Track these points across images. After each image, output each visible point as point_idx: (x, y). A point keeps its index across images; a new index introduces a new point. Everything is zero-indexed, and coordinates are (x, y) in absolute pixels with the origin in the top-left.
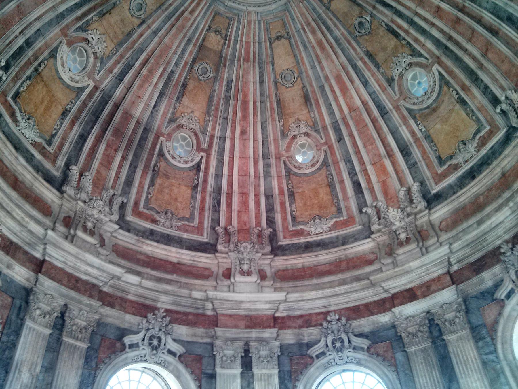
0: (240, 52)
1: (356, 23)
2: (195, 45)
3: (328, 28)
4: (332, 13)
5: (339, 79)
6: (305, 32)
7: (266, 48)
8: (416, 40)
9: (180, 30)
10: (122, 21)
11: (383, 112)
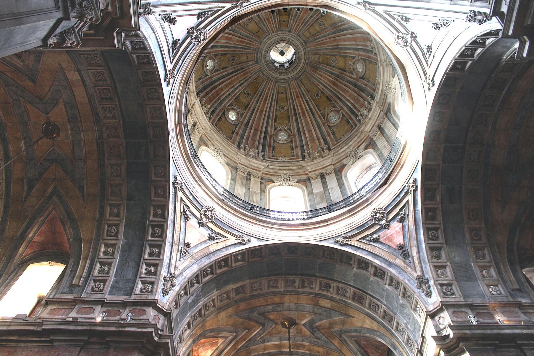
0: (272, 19)
1: (236, 58)
2: (293, 15)
4: (244, 54)
5: (230, 39)
7: (261, 26)
8: (218, 74)
9: (301, 19)
10: (326, 21)
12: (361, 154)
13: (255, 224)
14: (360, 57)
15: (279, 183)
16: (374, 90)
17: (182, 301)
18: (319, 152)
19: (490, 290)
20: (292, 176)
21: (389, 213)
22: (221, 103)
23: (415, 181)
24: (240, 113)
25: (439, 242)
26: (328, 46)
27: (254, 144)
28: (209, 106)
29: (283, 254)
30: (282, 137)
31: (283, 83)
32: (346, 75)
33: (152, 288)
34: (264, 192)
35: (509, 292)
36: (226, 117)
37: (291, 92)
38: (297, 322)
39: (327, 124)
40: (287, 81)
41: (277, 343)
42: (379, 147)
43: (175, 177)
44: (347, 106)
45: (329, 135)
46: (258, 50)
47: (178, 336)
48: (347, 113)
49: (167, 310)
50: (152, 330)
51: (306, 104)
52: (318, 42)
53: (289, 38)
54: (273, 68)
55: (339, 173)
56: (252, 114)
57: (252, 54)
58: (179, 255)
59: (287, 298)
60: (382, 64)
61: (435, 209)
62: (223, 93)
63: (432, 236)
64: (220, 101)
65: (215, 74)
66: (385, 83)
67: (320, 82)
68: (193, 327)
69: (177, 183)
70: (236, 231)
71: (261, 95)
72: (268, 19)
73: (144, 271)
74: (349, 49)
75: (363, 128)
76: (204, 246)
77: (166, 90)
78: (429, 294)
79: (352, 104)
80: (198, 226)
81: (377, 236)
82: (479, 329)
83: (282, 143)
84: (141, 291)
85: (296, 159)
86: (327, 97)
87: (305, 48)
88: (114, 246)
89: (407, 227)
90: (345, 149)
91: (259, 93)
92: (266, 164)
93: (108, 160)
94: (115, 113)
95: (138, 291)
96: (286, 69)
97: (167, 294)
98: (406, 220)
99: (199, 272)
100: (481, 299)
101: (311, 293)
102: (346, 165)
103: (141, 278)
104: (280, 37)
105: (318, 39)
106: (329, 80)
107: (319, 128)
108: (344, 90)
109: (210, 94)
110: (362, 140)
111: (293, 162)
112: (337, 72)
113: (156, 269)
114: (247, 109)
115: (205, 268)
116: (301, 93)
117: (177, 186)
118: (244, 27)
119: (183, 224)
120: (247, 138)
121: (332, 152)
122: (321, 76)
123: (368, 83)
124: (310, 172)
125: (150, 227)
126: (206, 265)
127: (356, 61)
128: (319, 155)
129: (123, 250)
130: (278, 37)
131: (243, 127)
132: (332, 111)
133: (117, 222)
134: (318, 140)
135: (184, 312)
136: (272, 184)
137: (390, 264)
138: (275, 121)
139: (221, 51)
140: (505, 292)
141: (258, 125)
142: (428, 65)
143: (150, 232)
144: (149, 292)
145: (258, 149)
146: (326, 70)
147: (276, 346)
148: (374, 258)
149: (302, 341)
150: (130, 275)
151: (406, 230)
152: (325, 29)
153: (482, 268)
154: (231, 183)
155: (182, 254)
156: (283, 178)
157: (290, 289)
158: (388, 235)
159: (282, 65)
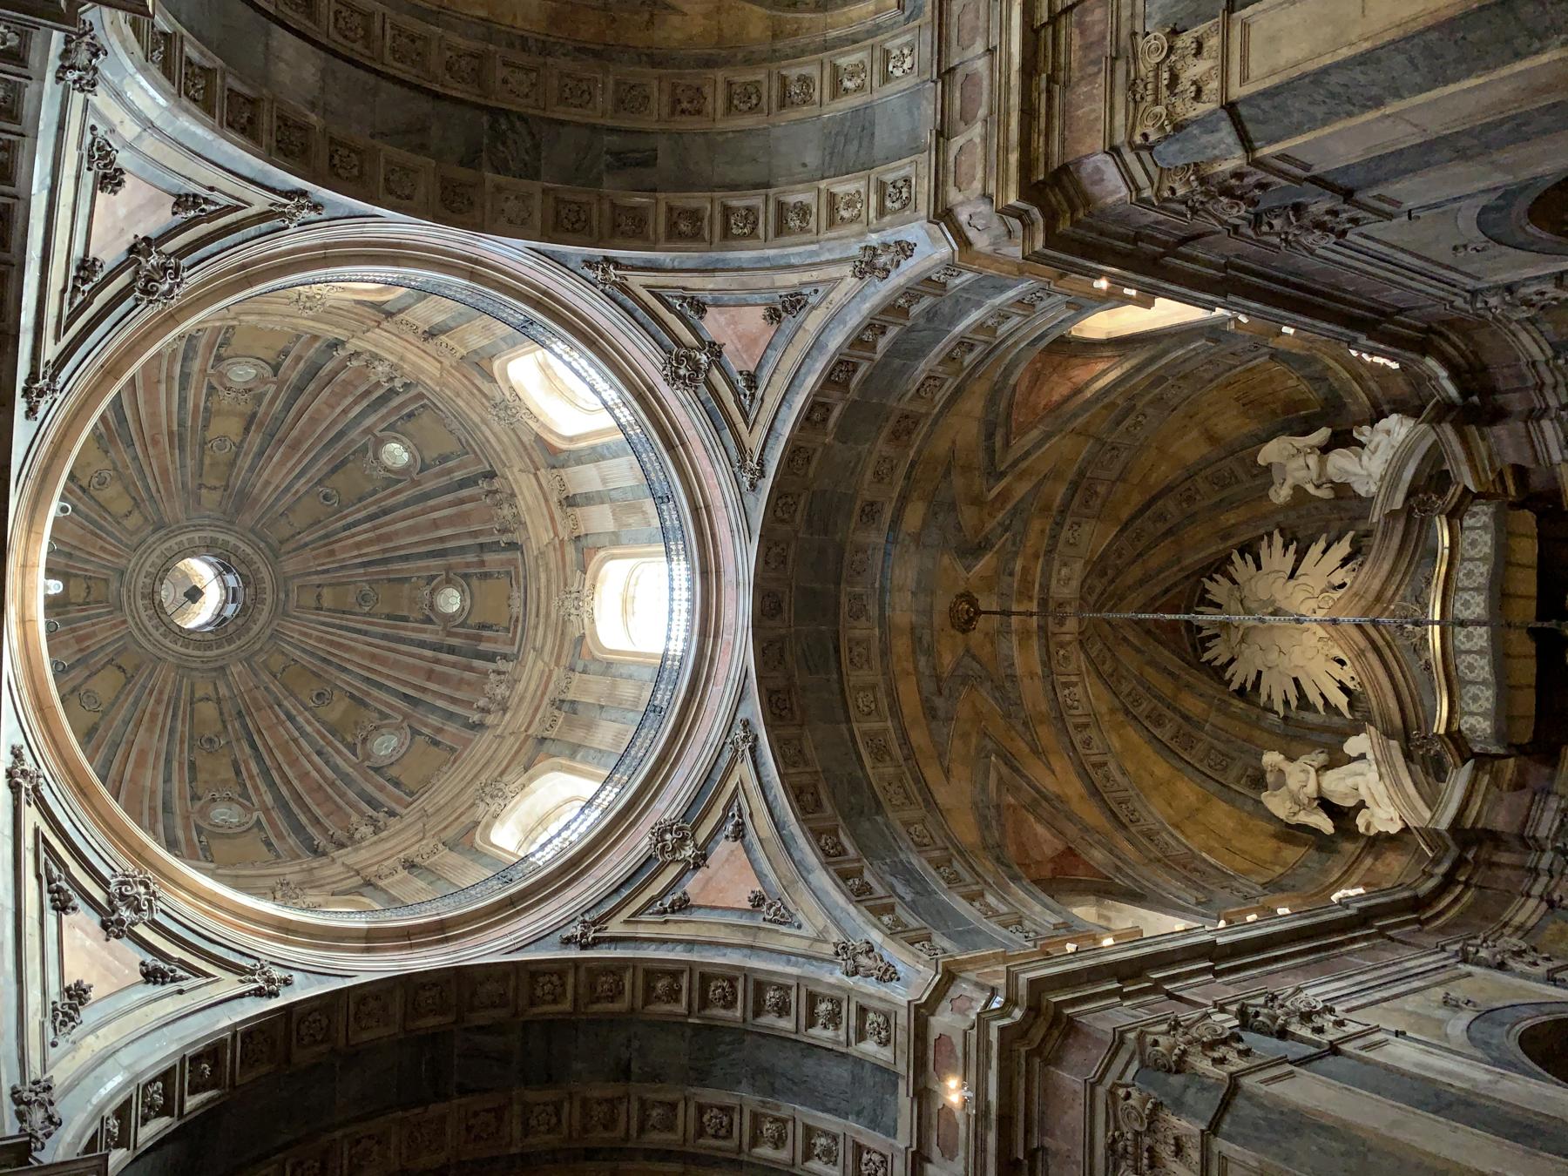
0: (81, 628)
1: (208, 734)
2: (67, 565)
3: (174, 716)
4: (192, 711)
5: (143, 754)
6: (151, 694)
8: (256, 788)
11: (167, 808)
12: (507, 394)
13: (701, 704)
14: (210, 371)
15: (586, 620)
16: (315, 338)
17: (914, 922)
18: (499, 504)
19: (898, 73)
20: (566, 585)
21: (678, 342)
22: (345, 778)
23: (589, 264)
24: (378, 722)
25: (762, 207)
26: (173, 462)
27: (469, 684)
28: (355, 818)
29: (783, 631)
30: (451, 601)
31: (287, 595)
32: (266, 414)
34: (610, 664)
35: (908, 20)
36: (387, 762)
37: (317, 573)
38: (961, 590)
39: (414, 475)
40: (282, 582)
41: (1015, 640)
42: (486, 342)
43: (567, 941)
44: (363, 414)
45: (450, 471)
46: (183, 667)
47: (1004, 932)
48: (383, 419)
49: (937, 973)
50: (995, 1025)
51: (353, 530)
52: (158, 491)
53: (143, 574)
54: (240, 621)
55: (562, 457)
56: (380, 686)
57: (193, 685)
58: (783, 929)
60: (232, 314)
61: (670, 209)
62: (314, 774)
63: (745, 226)
64: (338, 782)
65: (254, 798)
66: (293, 309)
67: (287, 489)
68: (978, 883)
69: (582, 936)
70: (720, 761)
71: (324, 660)
72: (79, 640)
74: (183, 400)
75: (431, 379)
76: (759, 854)
77: (303, 990)
78: (906, 249)
79: (355, 403)
80: (704, 868)
81: (739, 378)
82: (1008, 125)
83: (468, 601)
84: (884, 1043)
85: (516, 568)
86: (334, 470)
87: (180, 528)
88: (756, 1118)
89: (716, 294)
90: (494, 433)
91: (318, 663)
92: (532, 655)
93: (510, 1144)
94: (370, 1137)
95: (884, 1055)
96: (246, 584)
97: (891, 969)
98: (699, 295)
99: (831, 869)
100: (924, 102)
101: (887, 554)
102: (537, 434)
103: (848, 1044)
104: (140, 603)
105: (148, 489)
106: (282, 463)
107: (426, 496)
108: (314, 421)
109: (318, 811)
110: (466, 387)
111: (525, 578)
112: (255, 439)
114: (367, 700)
115: (820, 853)
116: (322, 542)
117: (591, 935)
118: (105, 713)
119: (697, 916)
120: (454, 700)
121: (498, 468)
122: (267, 483)
123: (293, 354)
124: (556, 534)
125: (708, 1012)
126: (813, 849)
127: (222, 384)
128: (506, 506)
129: (773, 1091)
130: (141, 610)
131: (419, 713)
132: (377, 458)
133: (692, 1111)
134: (462, 502)
135: (939, 912)
136: (588, 640)
137: (817, 345)
138: (405, 619)
139: (181, 780)
140: (905, 33)
141: (413, 670)
142: (238, 208)
143: (722, 1012)
144: (887, 1021)
145: (486, 674)
146: (252, 469)
148: (800, 387)
149: (1011, 574)
150: (842, 1072)
151: (726, 298)
152: (115, 469)
153: (837, 90)
154: (584, 761)
155: (784, 918)
156: (573, 611)
157: (873, 611)
158: (739, 347)
159: (231, 595)
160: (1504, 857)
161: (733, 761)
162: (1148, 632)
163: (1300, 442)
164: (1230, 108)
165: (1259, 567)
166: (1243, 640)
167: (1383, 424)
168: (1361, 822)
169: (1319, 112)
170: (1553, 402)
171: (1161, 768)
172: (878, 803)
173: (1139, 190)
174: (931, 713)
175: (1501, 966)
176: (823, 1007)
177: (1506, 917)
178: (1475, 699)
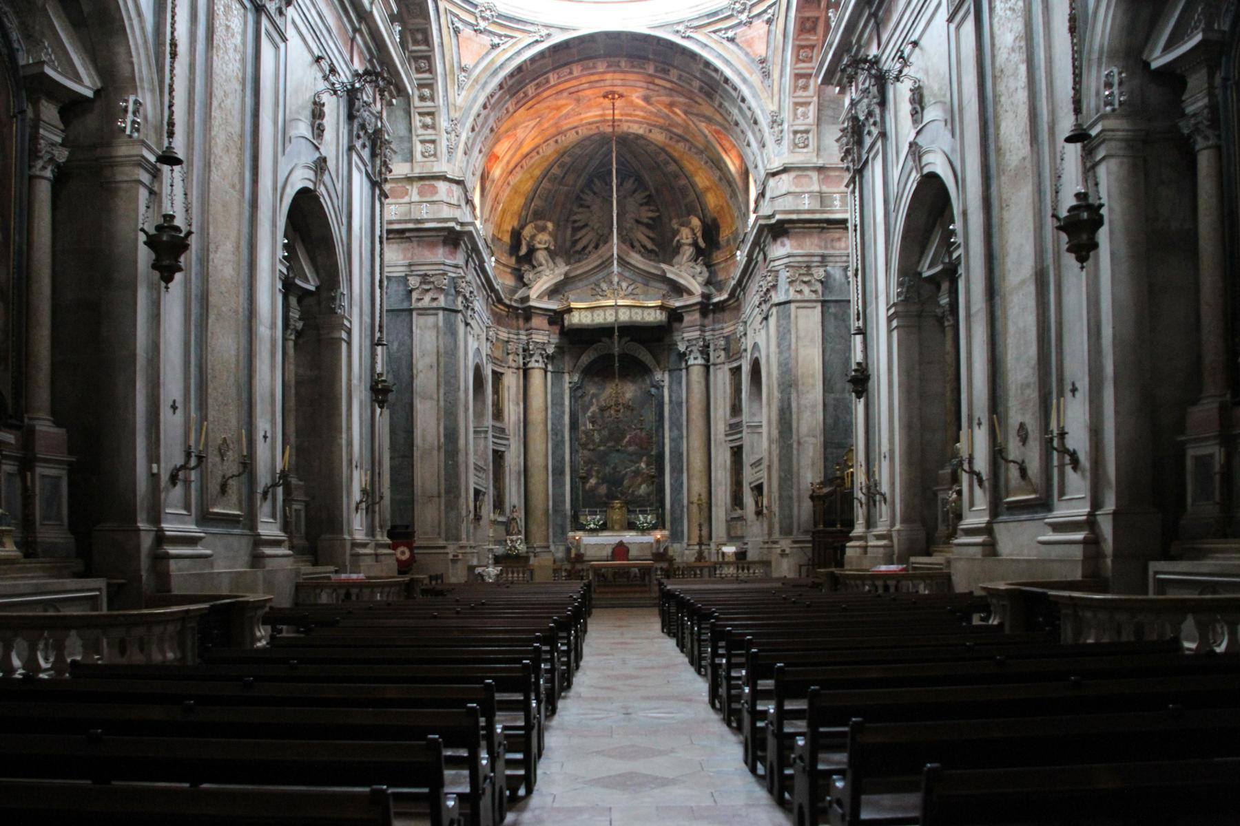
33: (435, 148)
58: (456, 87)
59: (608, 76)
73: (419, 124)
95: (418, 156)
103: (417, 136)
113: (433, 119)
119: (454, 41)
147: (596, 116)
150: (402, 131)
160: (521, 322)
161: (530, 32)
162: (606, 156)
163: (699, 234)
164: (789, 302)
165: (641, 205)
166: (603, 198)
167: (705, 269)
168: (526, 267)
169: (781, 329)
170: (707, 334)
171: (537, 173)
172: (514, 94)
173: (774, 261)
174: (562, 91)
175: (487, 339)
176: (428, 120)
177: (500, 328)
178: (586, 316)
